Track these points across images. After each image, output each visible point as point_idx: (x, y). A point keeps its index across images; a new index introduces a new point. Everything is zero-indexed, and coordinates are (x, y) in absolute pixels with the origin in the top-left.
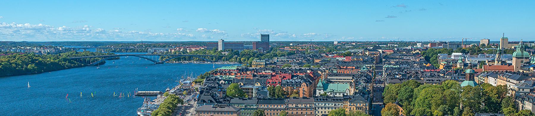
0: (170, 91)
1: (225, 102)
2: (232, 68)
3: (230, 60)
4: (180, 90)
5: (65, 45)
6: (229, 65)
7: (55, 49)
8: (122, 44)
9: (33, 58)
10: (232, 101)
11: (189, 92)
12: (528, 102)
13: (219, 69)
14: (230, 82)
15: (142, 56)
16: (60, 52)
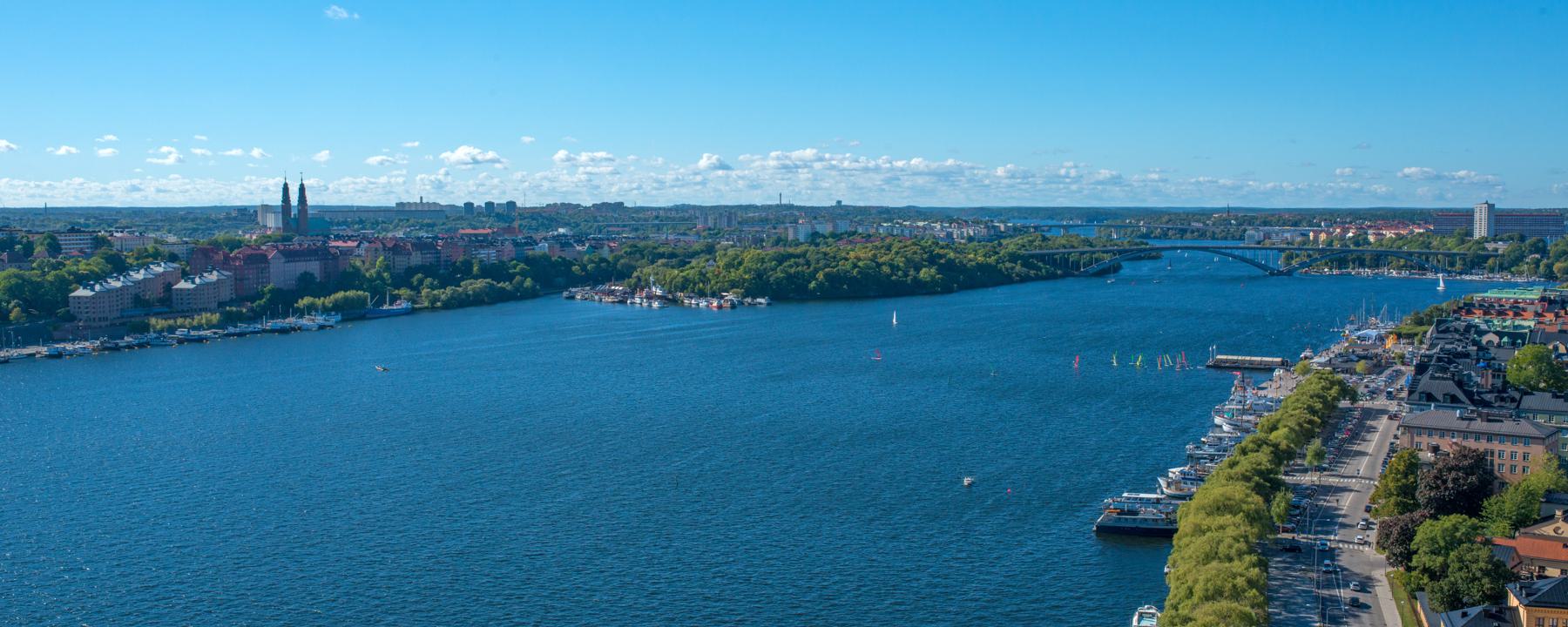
0: (1312, 358)
1: (1503, 404)
2: (1522, 296)
3: (1513, 269)
4: (1346, 357)
5: (1014, 218)
6: (1515, 285)
7: (987, 227)
8: (1169, 215)
9: (934, 251)
10: (1527, 402)
11: (1375, 366)
13: (1477, 297)
14: (1519, 341)
15: (1229, 251)
16: (1000, 236)
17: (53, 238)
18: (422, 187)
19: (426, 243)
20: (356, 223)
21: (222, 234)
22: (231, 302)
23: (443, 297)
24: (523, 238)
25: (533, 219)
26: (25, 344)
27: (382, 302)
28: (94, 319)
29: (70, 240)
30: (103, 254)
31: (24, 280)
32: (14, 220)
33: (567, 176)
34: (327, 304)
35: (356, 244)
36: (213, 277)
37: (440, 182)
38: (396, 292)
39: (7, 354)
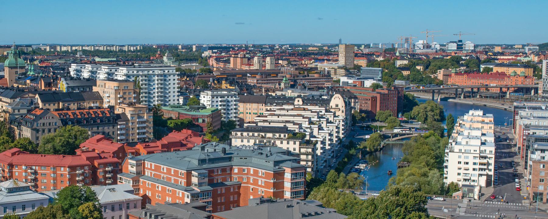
12: (25, 128)
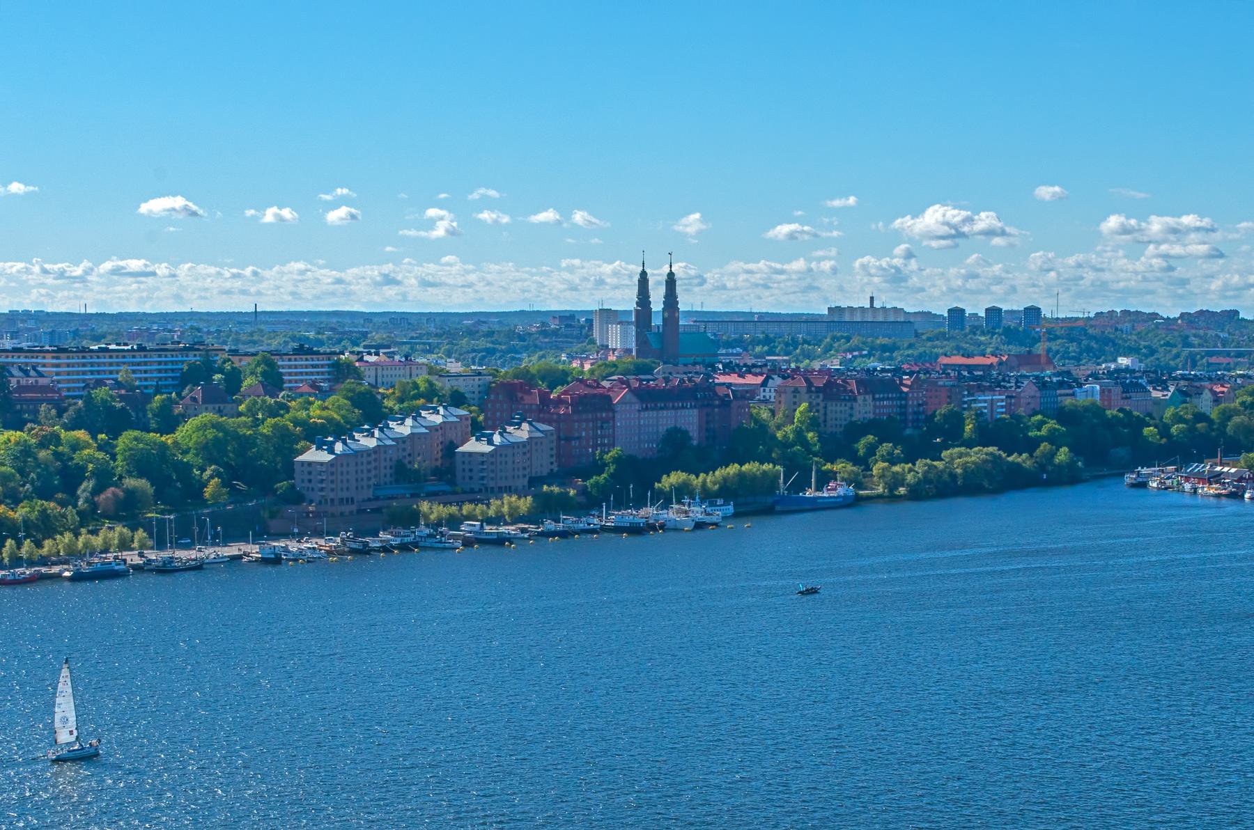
17: (271, 364)
18: (866, 280)
19: (882, 381)
20: (759, 342)
21: (534, 358)
22: (550, 478)
23: (910, 478)
24: (1054, 375)
25: (1072, 340)
26: (227, 539)
27: (803, 484)
28: (332, 500)
29: (296, 367)
30: (350, 390)
31: (226, 432)
32: (209, 333)
33: (1125, 261)
34: (709, 485)
35: (760, 380)
36: (523, 433)
37: (898, 270)
38: (829, 466)
39: (200, 555)
